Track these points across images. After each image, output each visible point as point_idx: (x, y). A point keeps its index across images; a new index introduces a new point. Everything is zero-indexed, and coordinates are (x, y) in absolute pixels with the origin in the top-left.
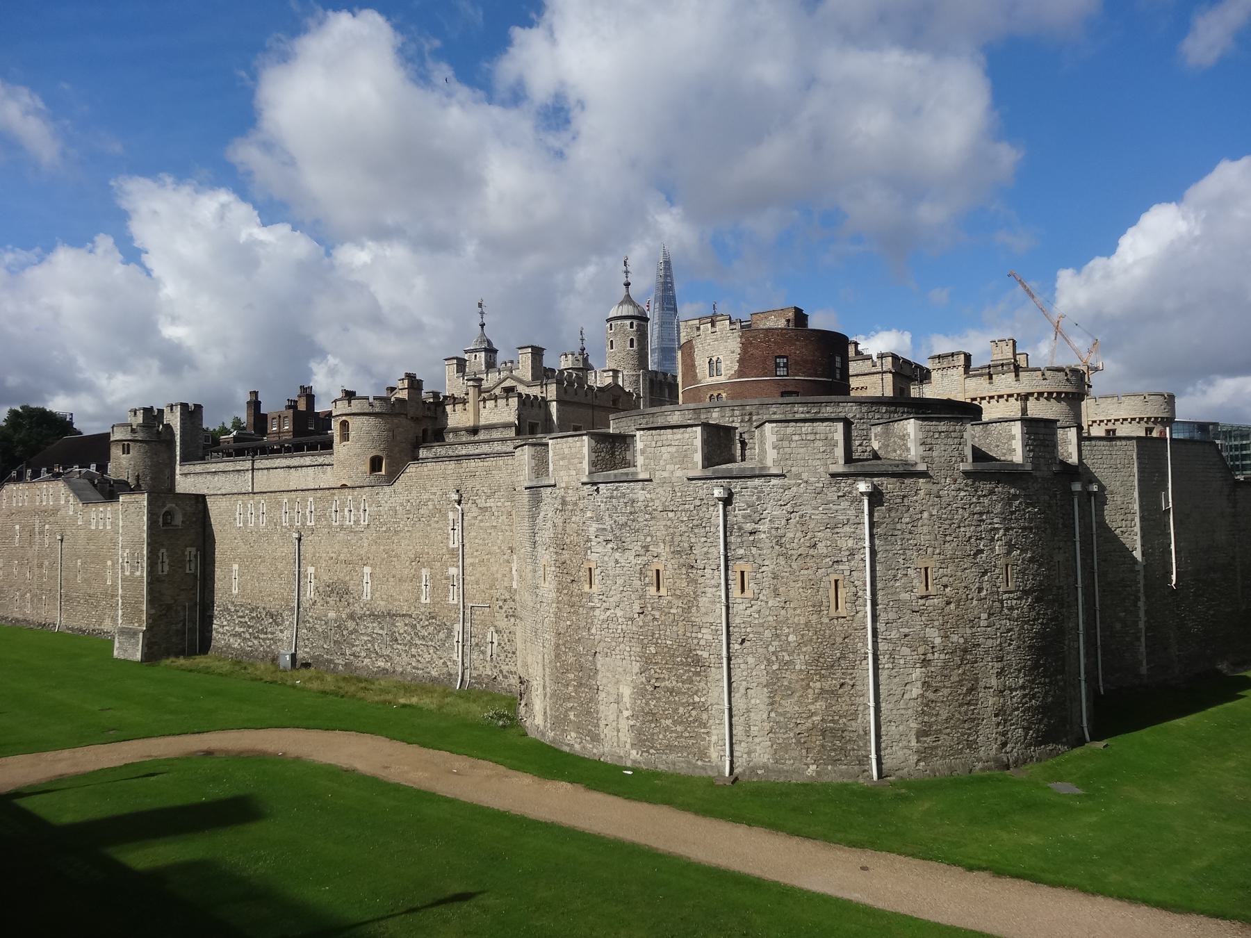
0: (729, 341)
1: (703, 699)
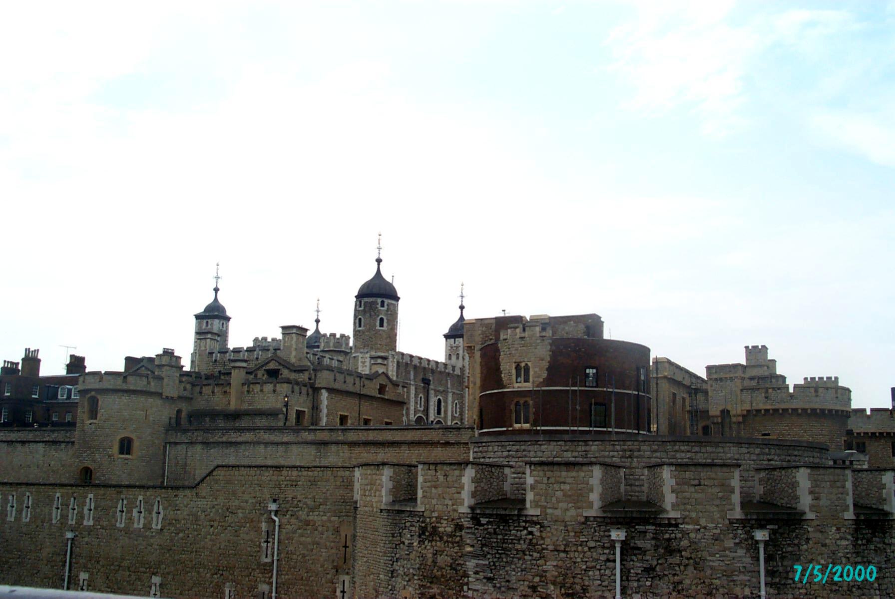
0: (538, 347)
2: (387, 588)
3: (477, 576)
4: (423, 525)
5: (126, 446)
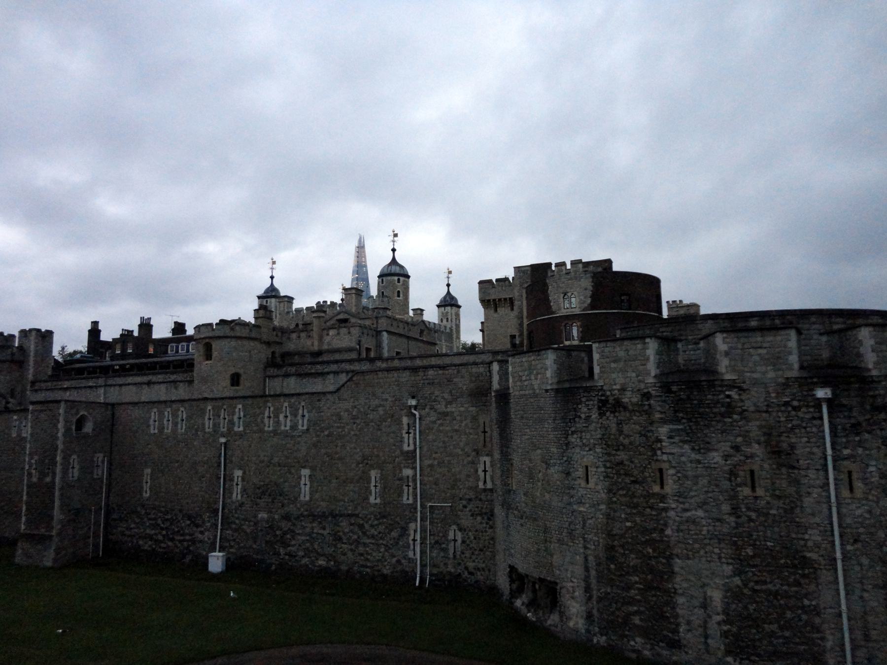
1: (814, 603)
2: (562, 459)
3: (672, 440)
4: (603, 398)
5: (235, 379)
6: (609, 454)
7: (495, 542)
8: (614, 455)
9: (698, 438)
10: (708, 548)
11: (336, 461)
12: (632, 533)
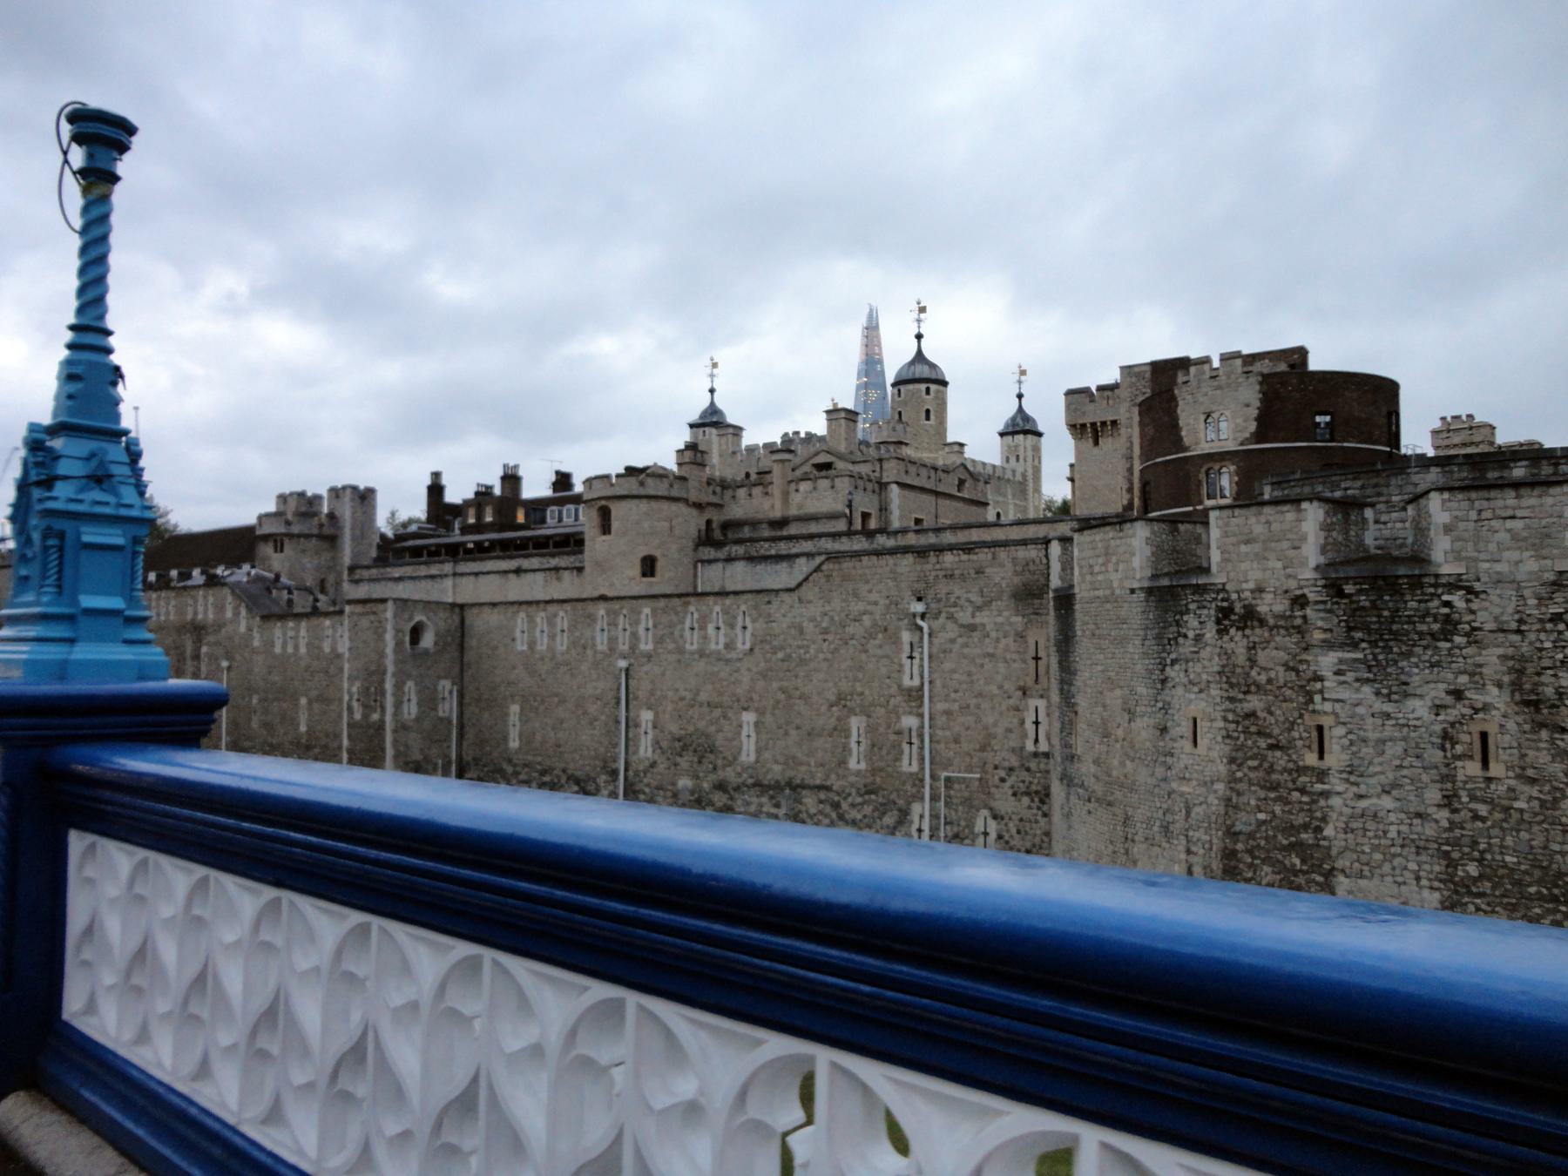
2: (1155, 706)
3: (1342, 678)
4: (1225, 604)
5: (649, 566)
6: (1231, 699)
7: (1050, 841)
8: (1240, 701)
9: (1390, 674)
10: (1397, 861)
11: (797, 701)
12: (1266, 831)
